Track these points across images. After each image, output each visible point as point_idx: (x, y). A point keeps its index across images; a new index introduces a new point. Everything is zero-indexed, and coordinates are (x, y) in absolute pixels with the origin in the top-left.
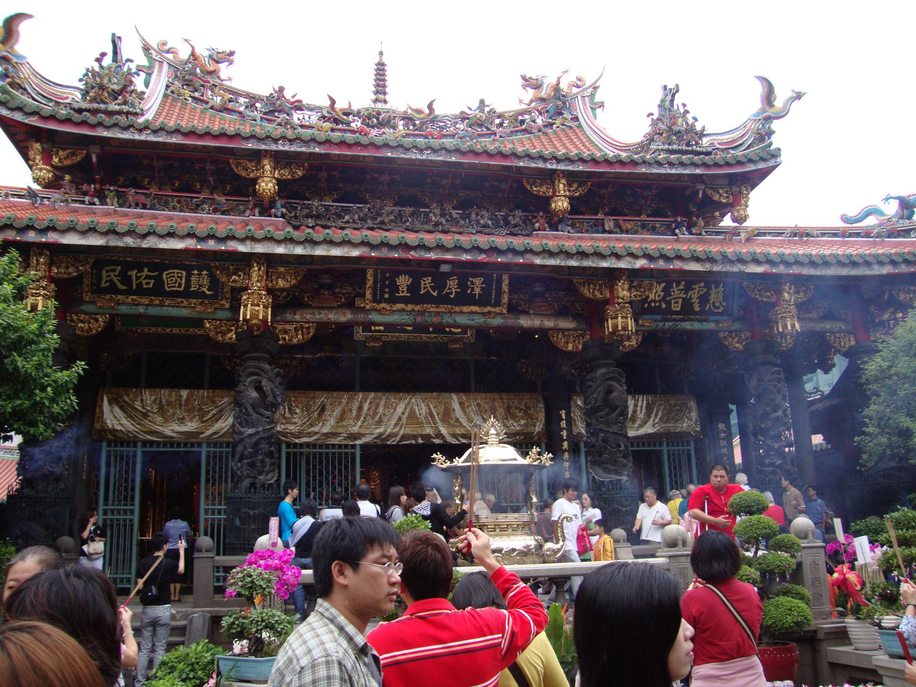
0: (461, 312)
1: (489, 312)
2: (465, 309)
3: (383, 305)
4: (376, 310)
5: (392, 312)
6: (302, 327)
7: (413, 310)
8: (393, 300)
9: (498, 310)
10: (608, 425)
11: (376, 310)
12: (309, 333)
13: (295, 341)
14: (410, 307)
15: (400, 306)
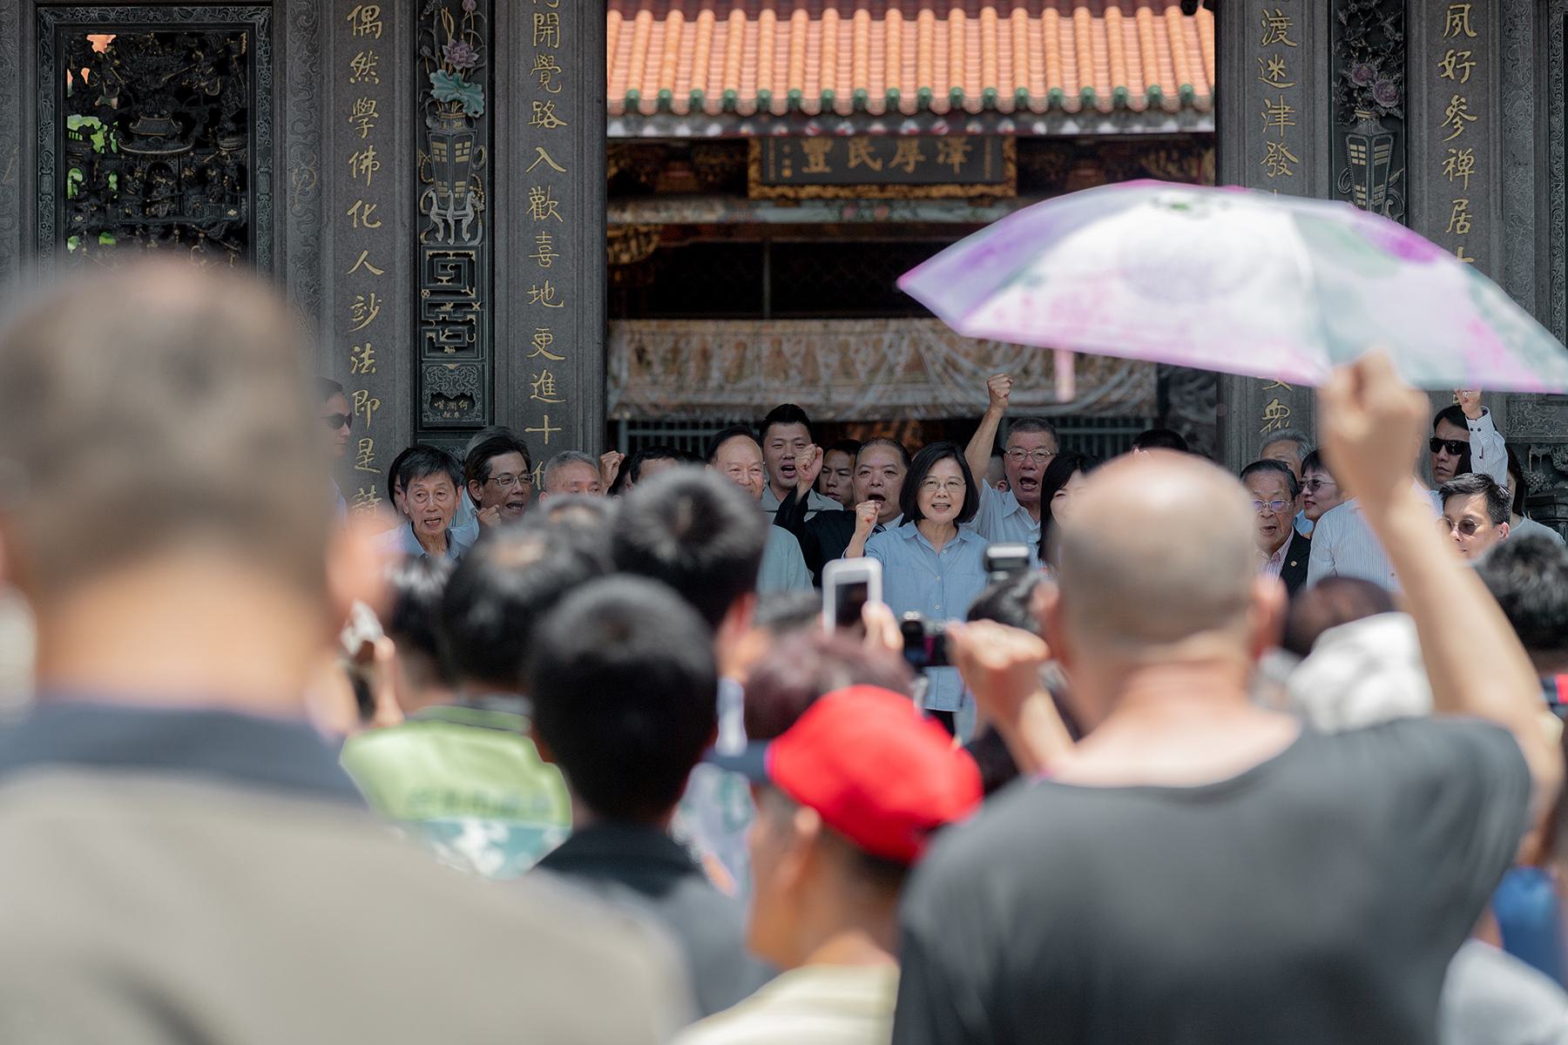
0: (928, 198)
1: (982, 196)
2: (935, 192)
3: (779, 190)
4: (769, 199)
5: (797, 202)
6: (637, 233)
7: (837, 198)
8: (799, 182)
9: (997, 190)
10: (1200, 410)
11: (769, 199)
12: (649, 243)
13: (625, 258)
14: (830, 192)
15: (812, 190)
